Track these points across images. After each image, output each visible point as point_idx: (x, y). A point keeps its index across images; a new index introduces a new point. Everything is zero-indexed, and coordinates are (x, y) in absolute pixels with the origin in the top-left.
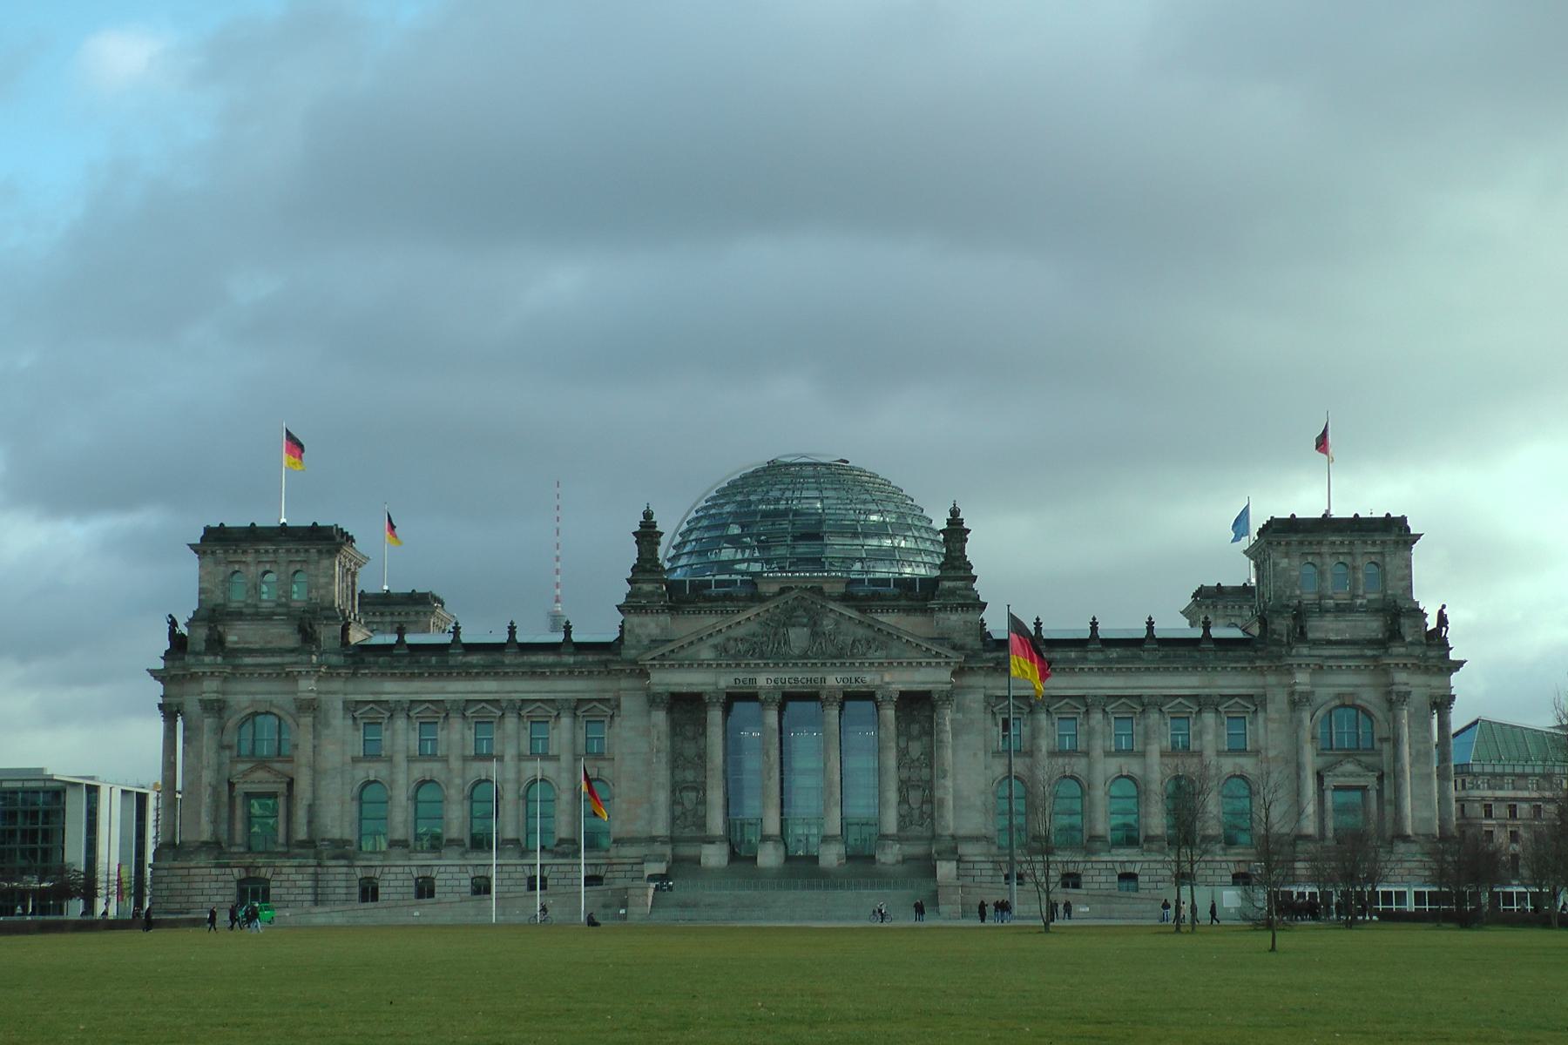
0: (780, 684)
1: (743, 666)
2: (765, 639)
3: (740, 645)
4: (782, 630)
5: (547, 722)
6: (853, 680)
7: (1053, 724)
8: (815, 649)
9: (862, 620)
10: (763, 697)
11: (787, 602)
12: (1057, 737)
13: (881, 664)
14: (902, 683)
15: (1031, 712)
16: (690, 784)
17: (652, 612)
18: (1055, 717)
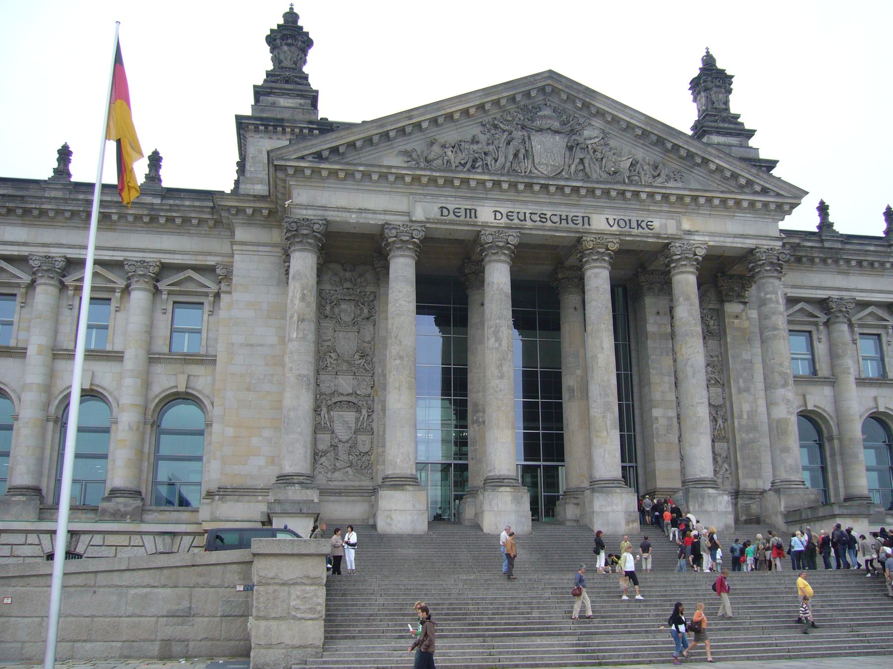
0: (516, 221)
1: (457, 183)
2: (491, 148)
3: (449, 153)
4: (520, 133)
5: (110, 299)
6: (634, 224)
7: (854, 342)
8: (573, 168)
9: (649, 129)
10: (487, 238)
11: (528, 94)
12: (860, 359)
13: (680, 198)
14: (712, 234)
15: (826, 324)
16: (346, 398)
17: (292, 130)
18: (857, 330)
